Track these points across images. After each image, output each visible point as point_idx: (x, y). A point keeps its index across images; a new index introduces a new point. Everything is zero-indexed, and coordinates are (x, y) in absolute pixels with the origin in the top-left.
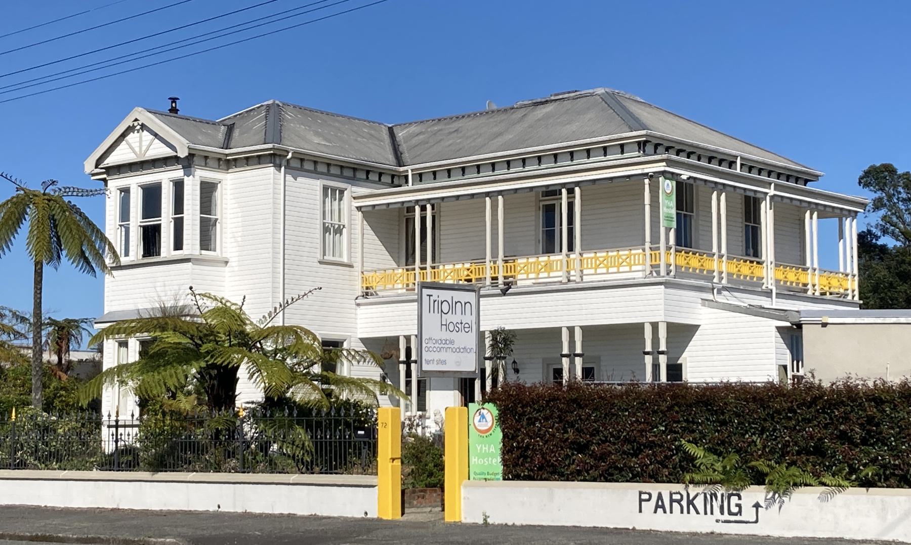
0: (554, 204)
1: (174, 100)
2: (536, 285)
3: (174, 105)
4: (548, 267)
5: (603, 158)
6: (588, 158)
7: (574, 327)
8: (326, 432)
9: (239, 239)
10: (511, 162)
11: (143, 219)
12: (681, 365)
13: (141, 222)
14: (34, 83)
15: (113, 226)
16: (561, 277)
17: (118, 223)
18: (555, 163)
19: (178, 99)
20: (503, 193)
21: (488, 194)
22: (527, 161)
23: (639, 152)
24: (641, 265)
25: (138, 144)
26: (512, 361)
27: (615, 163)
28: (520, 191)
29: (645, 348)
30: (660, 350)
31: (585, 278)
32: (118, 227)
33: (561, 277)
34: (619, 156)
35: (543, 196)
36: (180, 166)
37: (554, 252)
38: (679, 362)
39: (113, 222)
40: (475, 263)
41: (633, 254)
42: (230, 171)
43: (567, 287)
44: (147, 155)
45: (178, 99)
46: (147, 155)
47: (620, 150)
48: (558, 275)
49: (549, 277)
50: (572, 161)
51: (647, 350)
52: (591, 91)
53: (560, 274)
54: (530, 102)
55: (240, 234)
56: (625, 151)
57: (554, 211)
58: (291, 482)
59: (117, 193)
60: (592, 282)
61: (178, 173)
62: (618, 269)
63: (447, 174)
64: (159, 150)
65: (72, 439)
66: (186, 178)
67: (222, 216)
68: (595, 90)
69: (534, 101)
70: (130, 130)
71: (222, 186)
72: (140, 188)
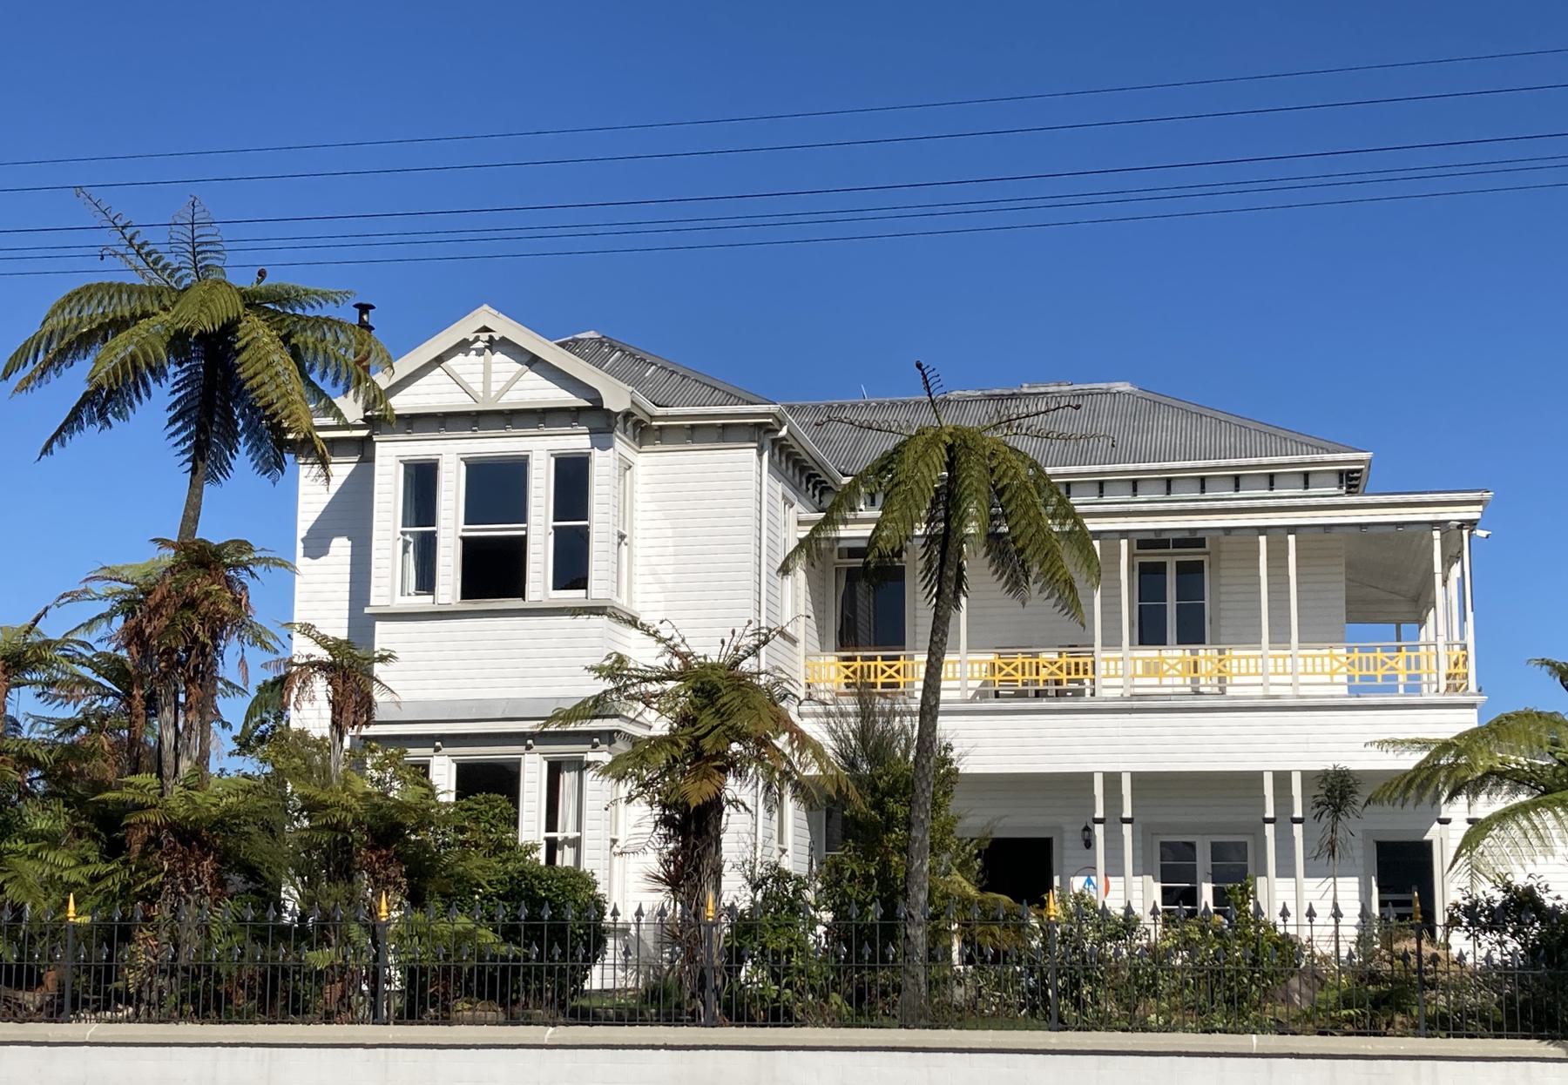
0: (1203, 561)
1: (364, 308)
2: (1135, 698)
3: (365, 317)
4: (1152, 669)
5: (1266, 493)
6: (1237, 490)
7: (1262, 772)
8: (550, 947)
9: (669, 578)
10: (1206, 480)
11: (466, 524)
12: (1430, 843)
13: (464, 530)
14: (1299, 183)
15: (389, 535)
16: (1104, 687)
17: (400, 528)
18: (1168, 494)
19: (373, 307)
20: (1299, 531)
21: (1262, 530)
22: (1139, 485)
23: (1340, 487)
24: (1288, 674)
25: (480, 378)
26: (1082, 827)
27: (1145, 507)
28: (1236, 532)
29: (1292, 813)
30: (1441, 817)
31: (1230, 691)
32: (399, 535)
33: (1104, 687)
34: (1300, 492)
35: (1138, 548)
36: (585, 429)
37: (1165, 644)
38: (1426, 838)
39: (390, 525)
40: (1023, 653)
41: (1235, 657)
42: (645, 448)
43: (1193, 704)
44: (504, 399)
45: (373, 307)
46: (504, 399)
47: (1233, 485)
48: (1176, 682)
49: (1161, 686)
50: (1203, 492)
51: (1267, 816)
52: (1104, 386)
53: (1179, 681)
54: (979, 393)
55: (670, 569)
56: (1310, 485)
57: (1165, 574)
58: (546, 1042)
59: (458, 466)
60: (1332, 696)
61: (577, 442)
62: (1332, 679)
63: (1164, 488)
64: (539, 392)
65: (1046, 958)
66: (596, 453)
67: (632, 532)
68: (1112, 385)
69: (987, 392)
70: (463, 346)
71: (632, 475)
72: (463, 463)
